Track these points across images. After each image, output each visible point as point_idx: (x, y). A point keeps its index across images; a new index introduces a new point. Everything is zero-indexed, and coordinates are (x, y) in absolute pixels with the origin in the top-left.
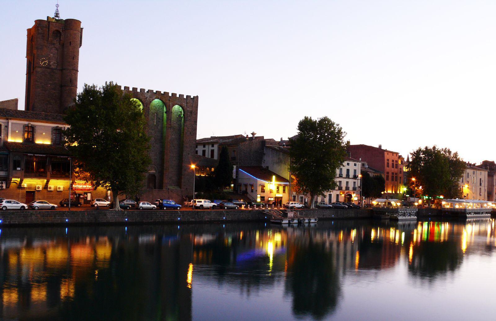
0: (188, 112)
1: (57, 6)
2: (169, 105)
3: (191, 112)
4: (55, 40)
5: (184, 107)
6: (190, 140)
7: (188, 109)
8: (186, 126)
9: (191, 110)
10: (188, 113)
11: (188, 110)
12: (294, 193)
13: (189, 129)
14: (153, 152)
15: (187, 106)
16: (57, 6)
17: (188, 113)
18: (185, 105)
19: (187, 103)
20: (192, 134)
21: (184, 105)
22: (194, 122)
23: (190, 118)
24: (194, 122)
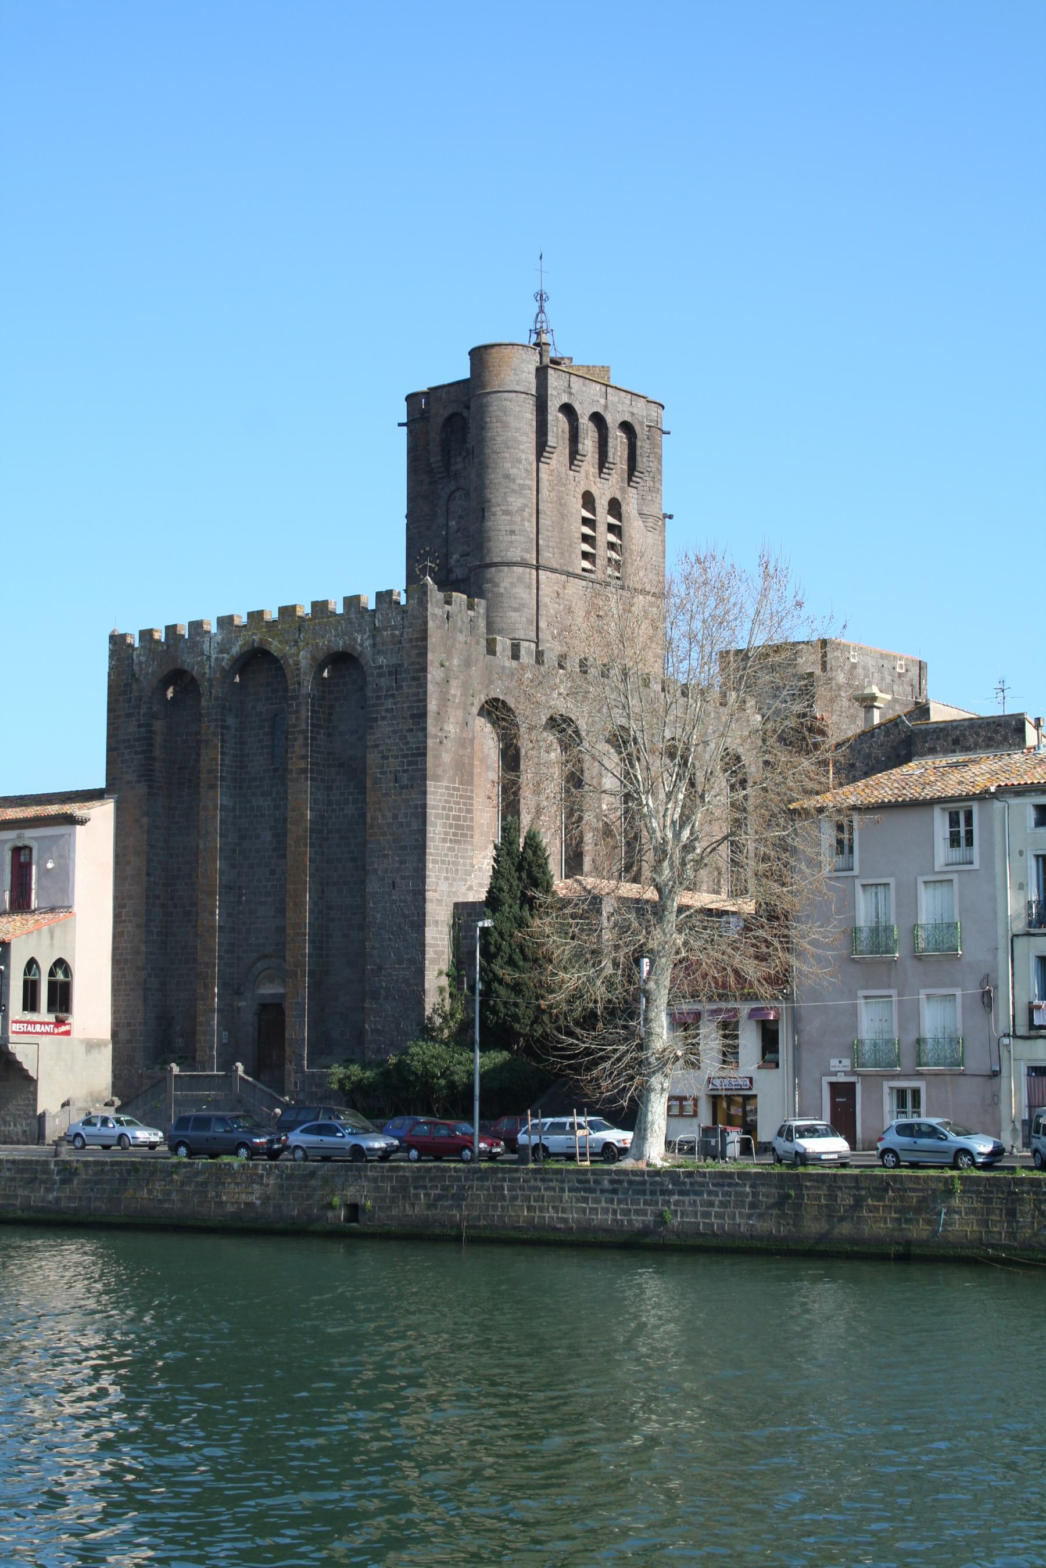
0: (380, 675)
1: (541, 297)
2: (297, 663)
3: (395, 671)
4: (459, 459)
5: (362, 653)
6: (395, 817)
7: (381, 660)
8: (376, 746)
9: (394, 661)
10: (383, 682)
11: (381, 667)
12: (834, 1062)
13: (387, 758)
14: (269, 899)
15: (374, 645)
16: (541, 297)
17: (383, 682)
18: (367, 643)
19: (375, 631)
20: (405, 782)
21: (361, 645)
22: (413, 716)
23: (389, 704)
24: (413, 716)
